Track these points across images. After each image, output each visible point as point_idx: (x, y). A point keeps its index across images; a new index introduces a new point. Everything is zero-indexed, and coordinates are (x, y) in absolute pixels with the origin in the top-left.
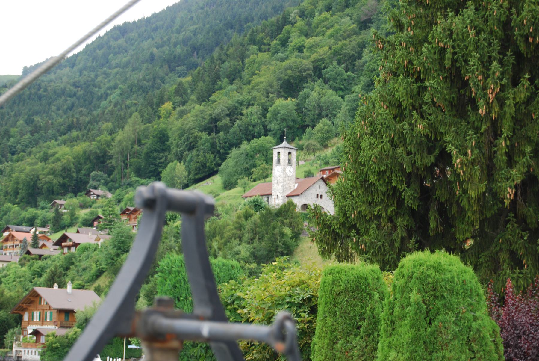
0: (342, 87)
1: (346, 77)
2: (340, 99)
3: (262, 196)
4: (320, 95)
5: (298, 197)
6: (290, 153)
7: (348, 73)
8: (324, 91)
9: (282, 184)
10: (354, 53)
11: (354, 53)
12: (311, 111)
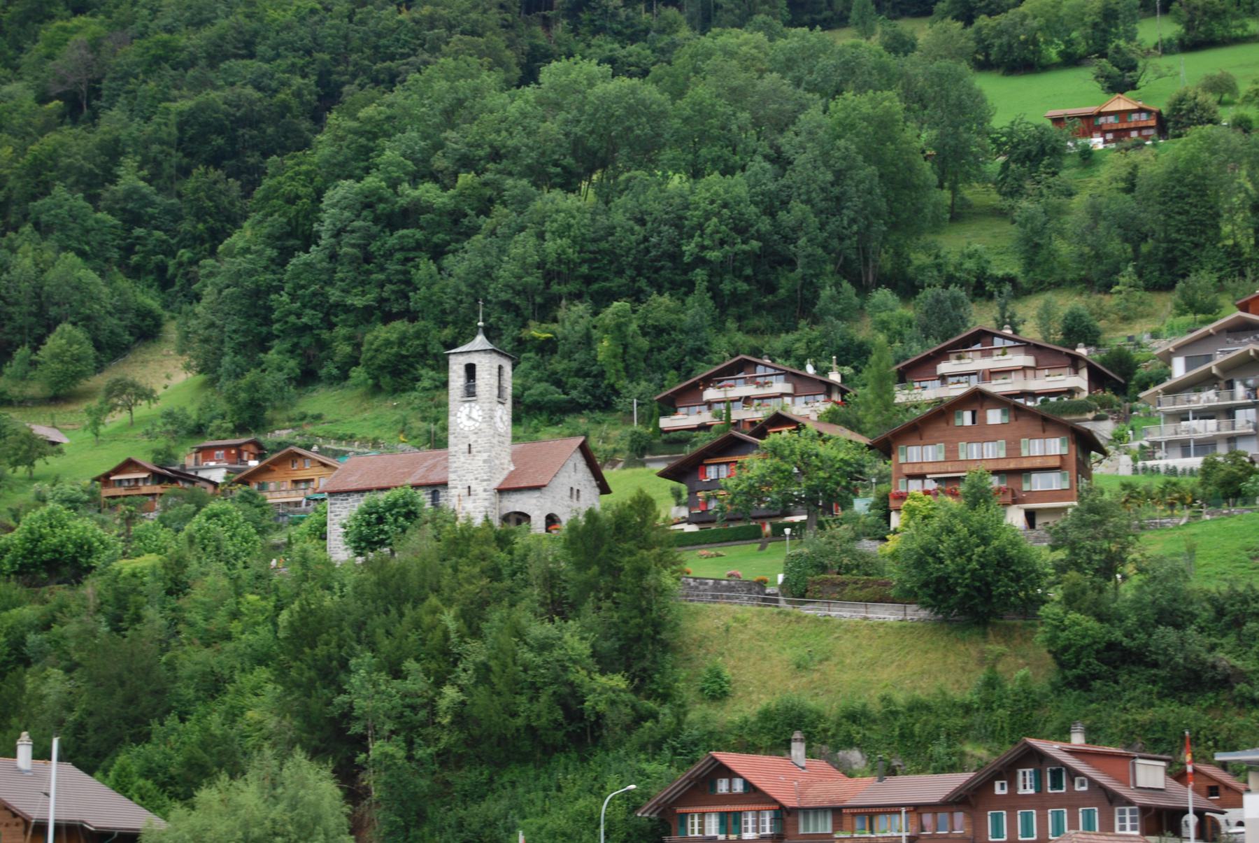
0: (87, 248)
1: (90, 223)
2: (93, 276)
3: (416, 487)
4: (37, 265)
5: (537, 494)
6: (500, 368)
7: (99, 215)
8: (46, 256)
9: (485, 456)
10: (92, 166)
11: (92, 166)
12: (17, 303)
